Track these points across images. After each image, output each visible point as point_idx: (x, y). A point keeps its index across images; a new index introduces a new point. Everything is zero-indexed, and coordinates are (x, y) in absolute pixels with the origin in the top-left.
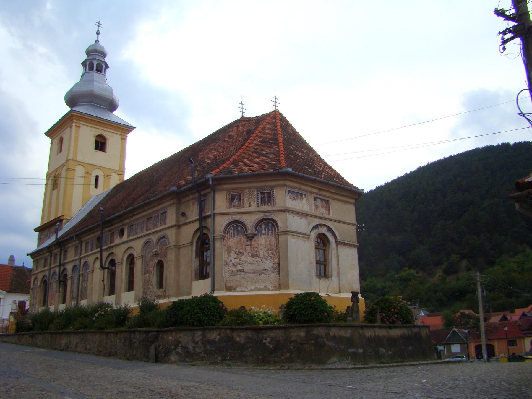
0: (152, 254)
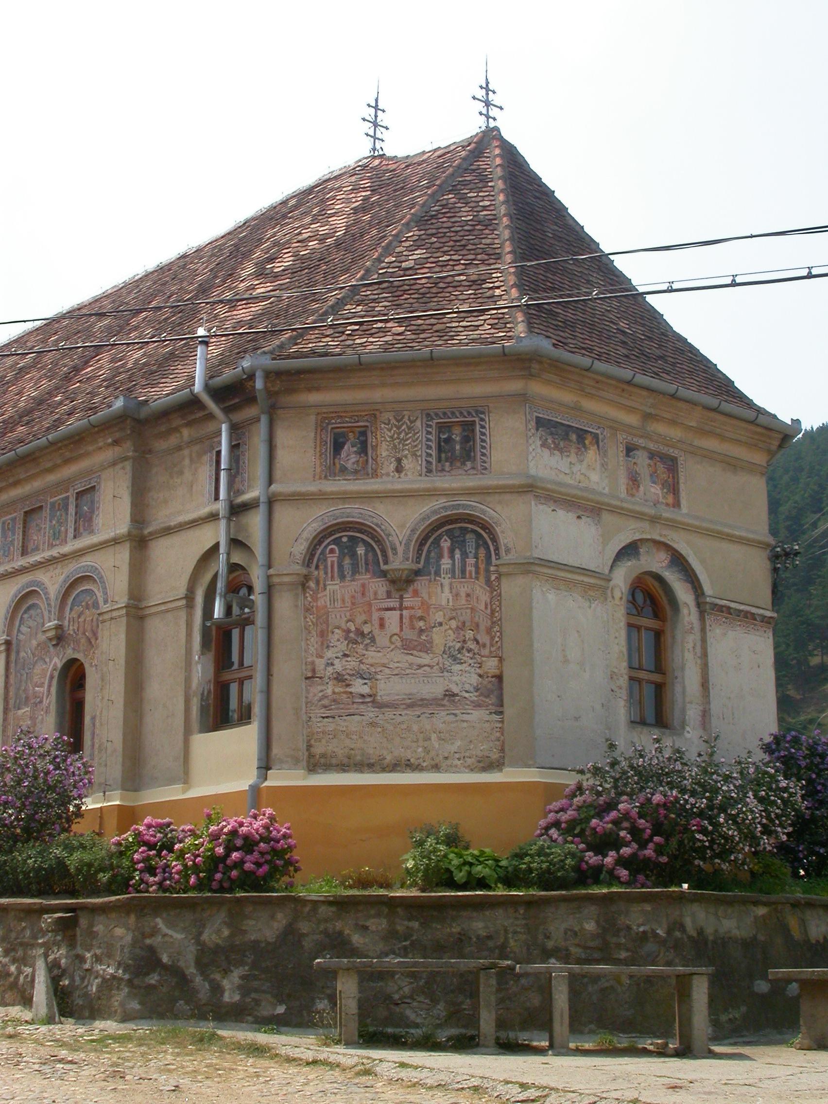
0: (42, 637)
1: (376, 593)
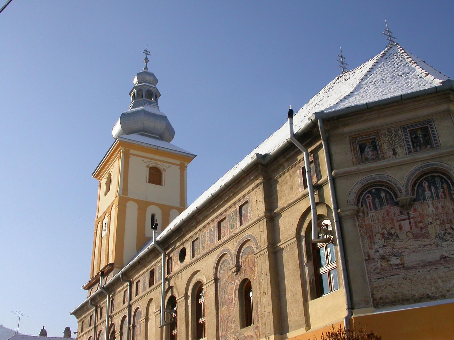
1: (394, 214)
